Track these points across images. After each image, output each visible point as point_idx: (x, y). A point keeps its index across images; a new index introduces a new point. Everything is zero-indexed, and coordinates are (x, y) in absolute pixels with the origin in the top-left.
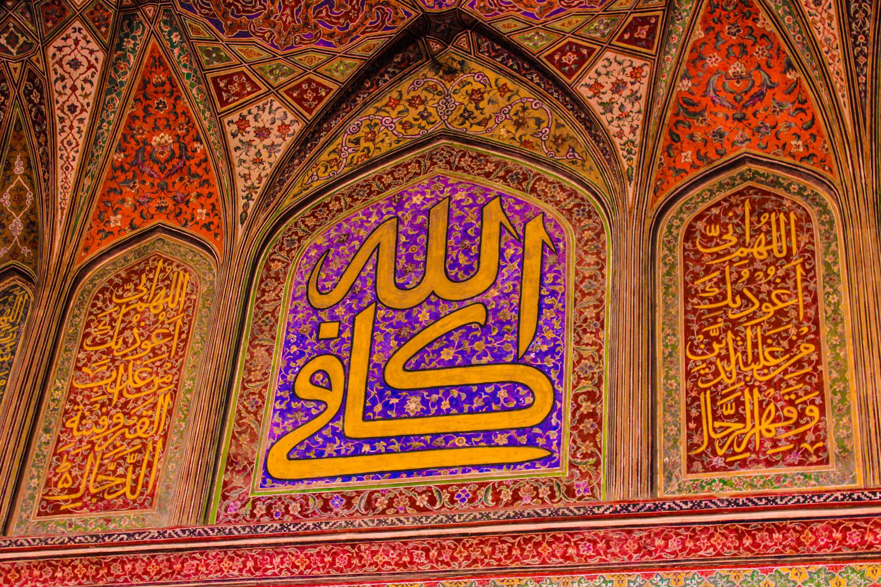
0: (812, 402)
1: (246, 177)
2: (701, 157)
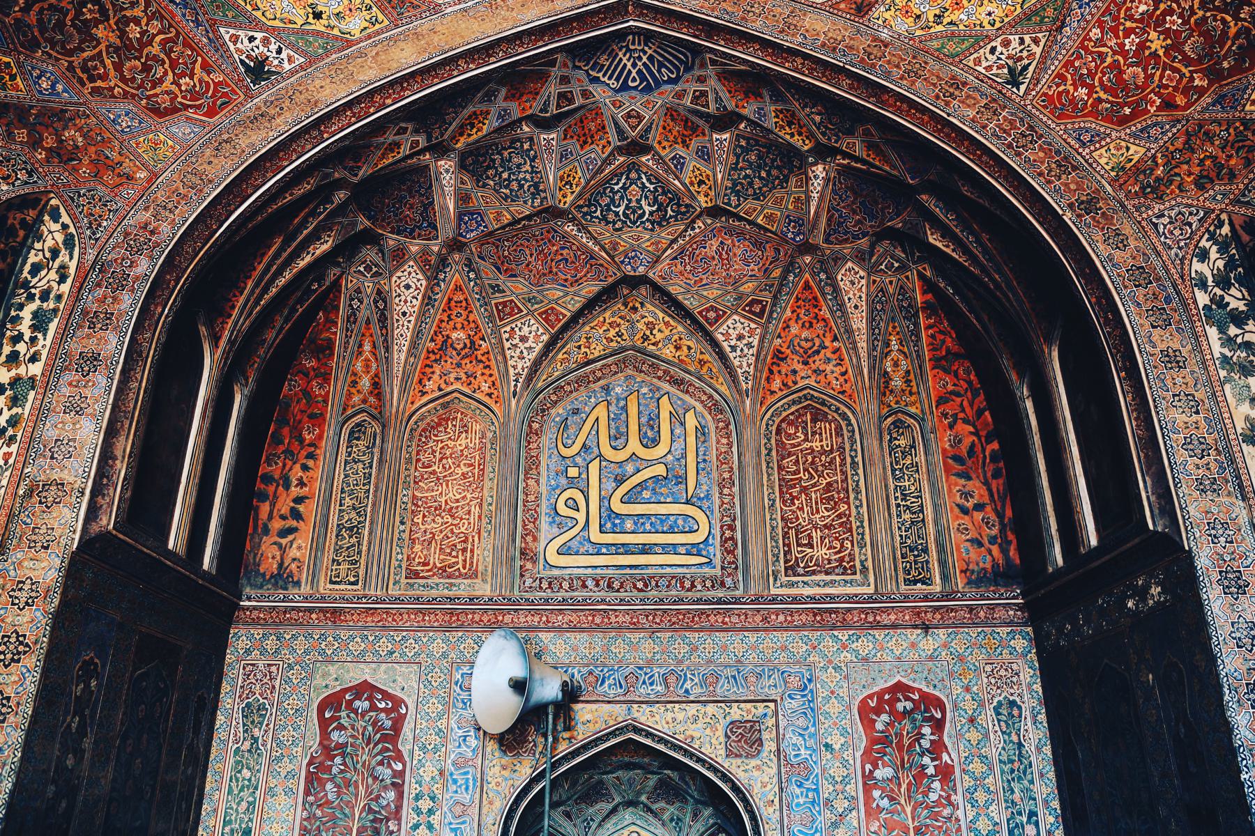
0: (847, 539)
1: (515, 367)
2: (785, 385)
